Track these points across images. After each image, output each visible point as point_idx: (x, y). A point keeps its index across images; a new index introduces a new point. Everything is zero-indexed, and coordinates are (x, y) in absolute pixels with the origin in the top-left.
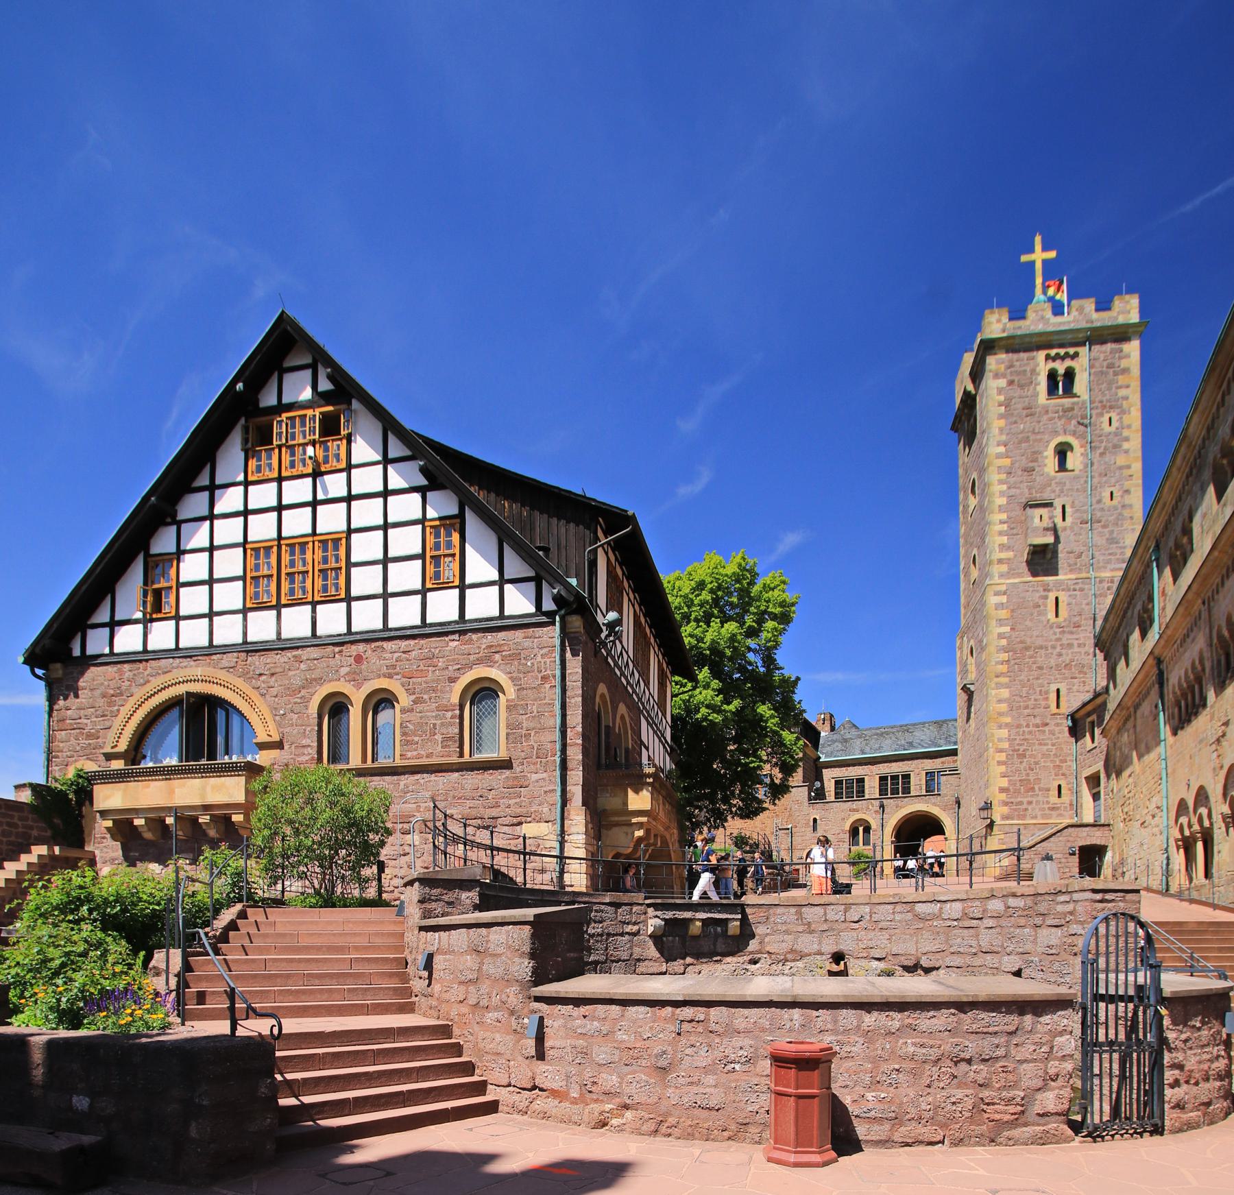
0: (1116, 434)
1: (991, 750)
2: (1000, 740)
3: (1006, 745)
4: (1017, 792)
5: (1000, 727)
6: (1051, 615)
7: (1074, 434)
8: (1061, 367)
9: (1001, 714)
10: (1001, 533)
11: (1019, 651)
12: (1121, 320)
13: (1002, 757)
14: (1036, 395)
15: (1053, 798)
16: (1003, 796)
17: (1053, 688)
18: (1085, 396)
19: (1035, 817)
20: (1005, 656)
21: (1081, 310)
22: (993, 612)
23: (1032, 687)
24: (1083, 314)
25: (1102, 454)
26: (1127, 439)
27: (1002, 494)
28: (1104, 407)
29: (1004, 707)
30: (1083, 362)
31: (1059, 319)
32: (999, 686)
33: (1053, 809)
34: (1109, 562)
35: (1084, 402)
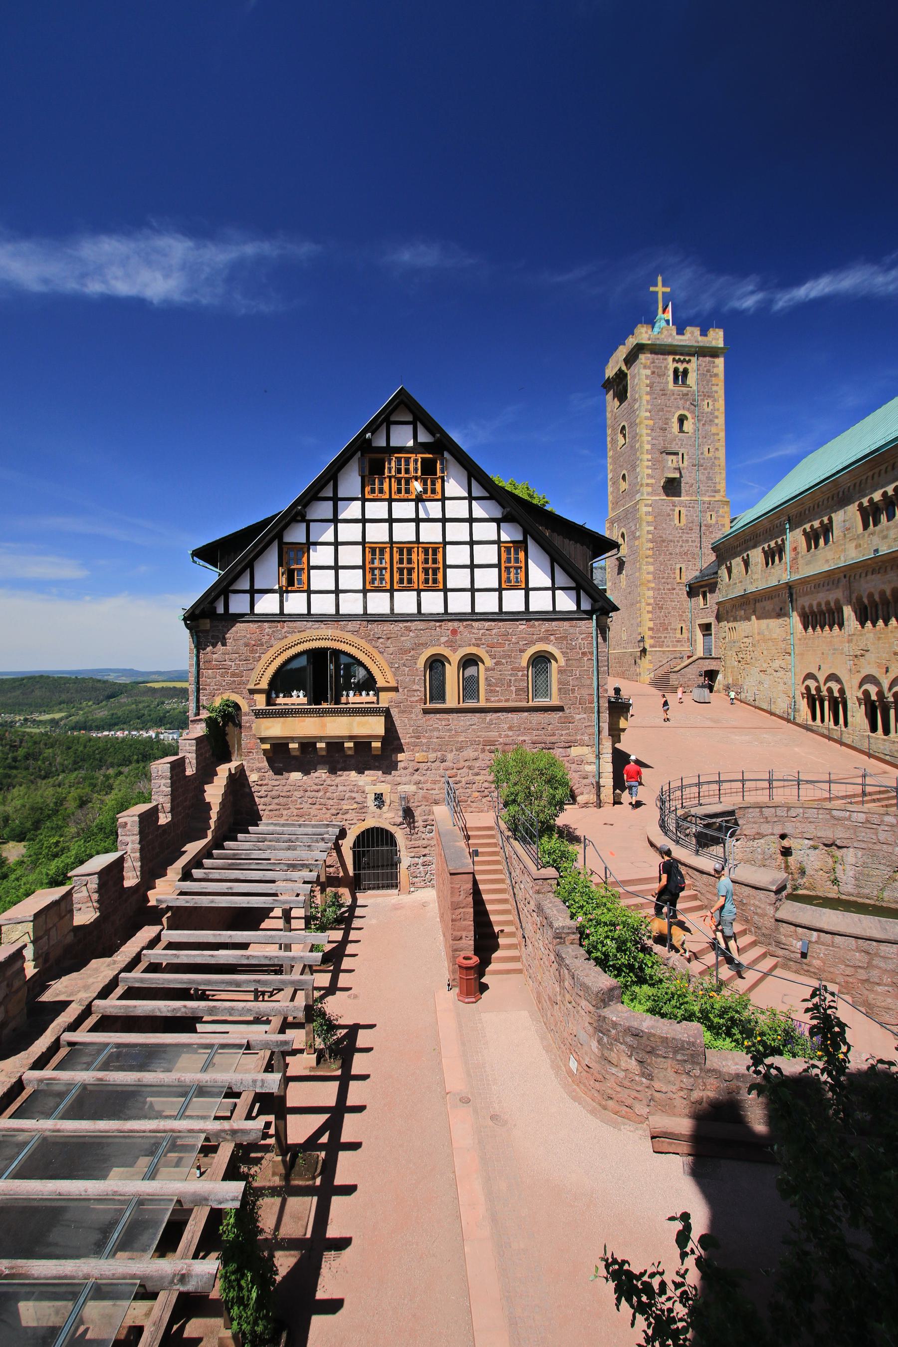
0: (711, 413)
1: (643, 604)
2: (649, 597)
3: (652, 601)
4: (658, 630)
5: (648, 590)
6: (677, 521)
7: (688, 410)
8: (681, 367)
9: (649, 581)
10: (648, 467)
11: (659, 542)
12: (714, 344)
13: (650, 608)
14: (667, 383)
15: (678, 635)
16: (650, 633)
17: (678, 566)
18: (695, 388)
19: (668, 646)
20: (651, 545)
21: (692, 333)
22: (644, 517)
23: (666, 565)
24: (692, 337)
25: (704, 425)
26: (717, 417)
27: (648, 442)
28: (705, 396)
29: (650, 577)
30: (693, 365)
31: (680, 337)
32: (648, 563)
33: (678, 641)
34: (707, 491)
35: (694, 391)
